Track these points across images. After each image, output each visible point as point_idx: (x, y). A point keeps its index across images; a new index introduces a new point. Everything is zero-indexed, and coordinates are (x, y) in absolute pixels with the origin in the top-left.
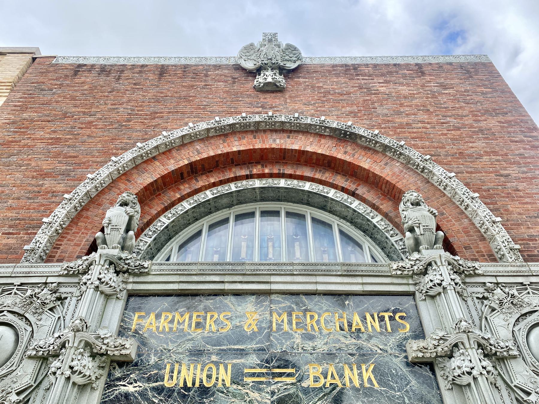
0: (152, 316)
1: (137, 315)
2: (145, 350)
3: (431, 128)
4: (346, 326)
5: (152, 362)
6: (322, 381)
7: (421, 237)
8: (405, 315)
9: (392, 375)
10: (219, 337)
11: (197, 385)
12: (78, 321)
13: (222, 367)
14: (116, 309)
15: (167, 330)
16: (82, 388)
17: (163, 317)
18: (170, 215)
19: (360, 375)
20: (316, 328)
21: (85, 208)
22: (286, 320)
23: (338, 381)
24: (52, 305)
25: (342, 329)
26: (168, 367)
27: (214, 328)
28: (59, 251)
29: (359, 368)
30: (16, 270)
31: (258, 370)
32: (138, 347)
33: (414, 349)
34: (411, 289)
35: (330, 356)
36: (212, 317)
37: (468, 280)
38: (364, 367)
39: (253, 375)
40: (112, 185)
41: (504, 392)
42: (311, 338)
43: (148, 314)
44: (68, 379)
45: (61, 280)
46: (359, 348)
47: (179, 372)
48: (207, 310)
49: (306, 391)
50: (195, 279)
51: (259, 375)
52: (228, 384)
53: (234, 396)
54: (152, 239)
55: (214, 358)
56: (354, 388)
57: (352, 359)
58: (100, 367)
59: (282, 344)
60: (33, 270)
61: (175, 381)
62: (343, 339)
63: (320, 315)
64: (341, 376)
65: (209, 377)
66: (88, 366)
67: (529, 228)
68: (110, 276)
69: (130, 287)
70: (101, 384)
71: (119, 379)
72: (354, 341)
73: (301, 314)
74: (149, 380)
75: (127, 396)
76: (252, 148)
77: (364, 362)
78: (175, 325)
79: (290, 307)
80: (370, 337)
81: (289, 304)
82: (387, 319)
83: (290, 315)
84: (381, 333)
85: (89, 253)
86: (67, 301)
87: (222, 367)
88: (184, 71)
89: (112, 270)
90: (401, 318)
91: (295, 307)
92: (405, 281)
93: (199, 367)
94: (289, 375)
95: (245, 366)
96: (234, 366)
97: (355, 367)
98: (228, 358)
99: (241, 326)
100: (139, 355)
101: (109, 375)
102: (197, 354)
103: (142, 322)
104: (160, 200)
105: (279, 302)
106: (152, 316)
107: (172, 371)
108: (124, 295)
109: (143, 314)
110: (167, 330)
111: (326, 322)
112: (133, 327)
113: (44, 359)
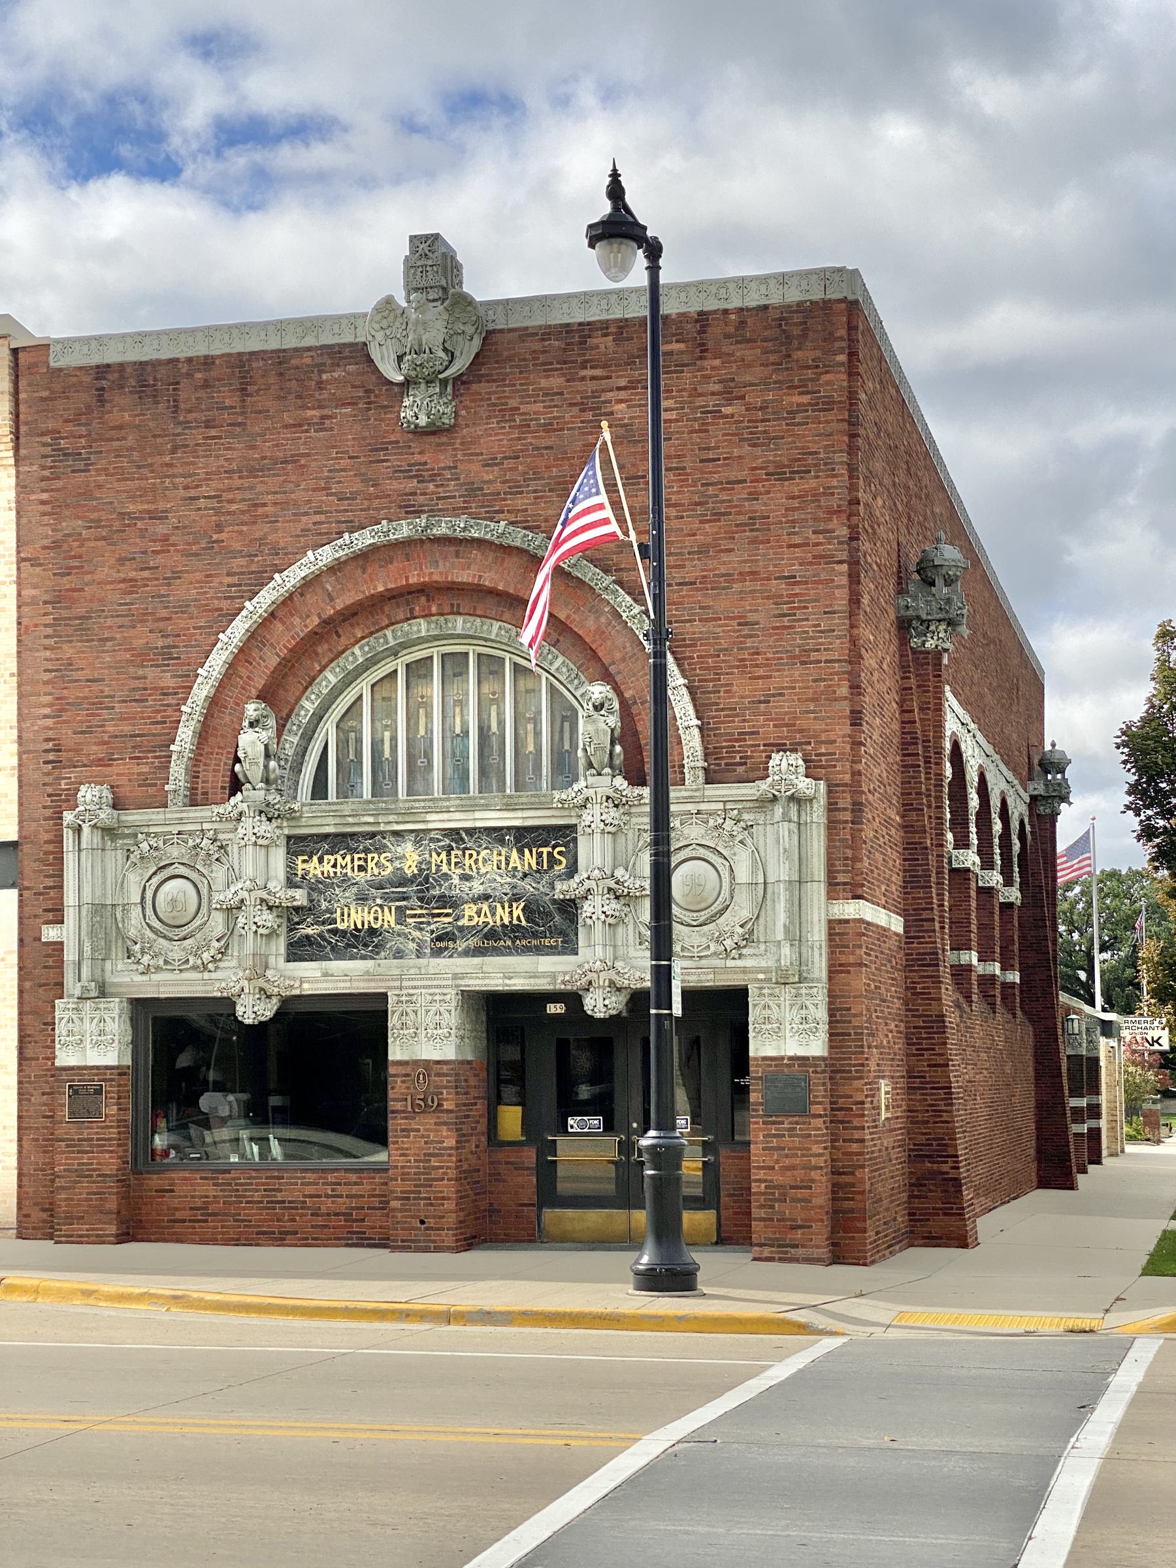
0: (315, 858)
1: (301, 858)
2: (315, 895)
3: (677, 518)
4: (503, 865)
5: (323, 907)
6: (476, 919)
7: (592, 759)
8: (563, 849)
9: (540, 912)
10: (380, 883)
11: (366, 926)
12: (248, 882)
13: (386, 909)
14: (279, 857)
15: (332, 875)
16: (269, 936)
17: (326, 861)
18: (313, 697)
19: (511, 913)
20: (474, 867)
21: (207, 716)
22: (445, 861)
23: (490, 920)
24: (216, 856)
25: (499, 868)
26: (339, 911)
27: (376, 871)
28: (200, 781)
29: (511, 906)
30: (169, 816)
31: (419, 912)
32: (309, 894)
33: (563, 890)
34: (574, 821)
35: (486, 897)
36: (373, 859)
37: (633, 810)
38: (515, 905)
39: (414, 916)
40: (230, 672)
41: (631, 927)
42: (465, 878)
43: (311, 857)
44: (256, 932)
45: (216, 826)
46: (514, 887)
47: (349, 915)
48: (366, 851)
49: (461, 929)
50: (350, 820)
51: (420, 916)
52: (393, 925)
53: (399, 935)
54: (297, 738)
55: (379, 901)
56: (503, 925)
57: (506, 898)
58: (278, 916)
59: (441, 886)
60: (184, 815)
61: (346, 924)
62: (499, 879)
63: (478, 853)
64: (493, 914)
65: (376, 919)
66: (268, 918)
67: (744, 721)
68: (265, 828)
69: (286, 832)
70: (284, 929)
71: (298, 923)
72: (509, 880)
73: (460, 853)
74: (323, 923)
75: (308, 937)
76: (404, 583)
77: (516, 901)
78: (339, 870)
79: (450, 846)
80: (525, 875)
81: (448, 842)
82: (545, 856)
83: (449, 854)
84: (538, 871)
85: (233, 794)
86: (229, 849)
87: (386, 909)
88: (281, 374)
89: (264, 818)
90: (560, 853)
91: (454, 845)
92: (566, 813)
93: (366, 909)
94: (447, 915)
95: (407, 908)
96: (397, 908)
97: (506, 905)
98: (392, 901)
99: (401, 869)
100: (311, 901)
101: (289, 920)
102: (362, 899)
103: (305, 866)
104: (295, 675)
105: (439, 840)
106: (315, 858)
107: (343, 915)
108: (282, 842)
109: (306, 858)
110: (332, 875)
111: (485, 861)
112: (300, 873)
113: (232, 911)
